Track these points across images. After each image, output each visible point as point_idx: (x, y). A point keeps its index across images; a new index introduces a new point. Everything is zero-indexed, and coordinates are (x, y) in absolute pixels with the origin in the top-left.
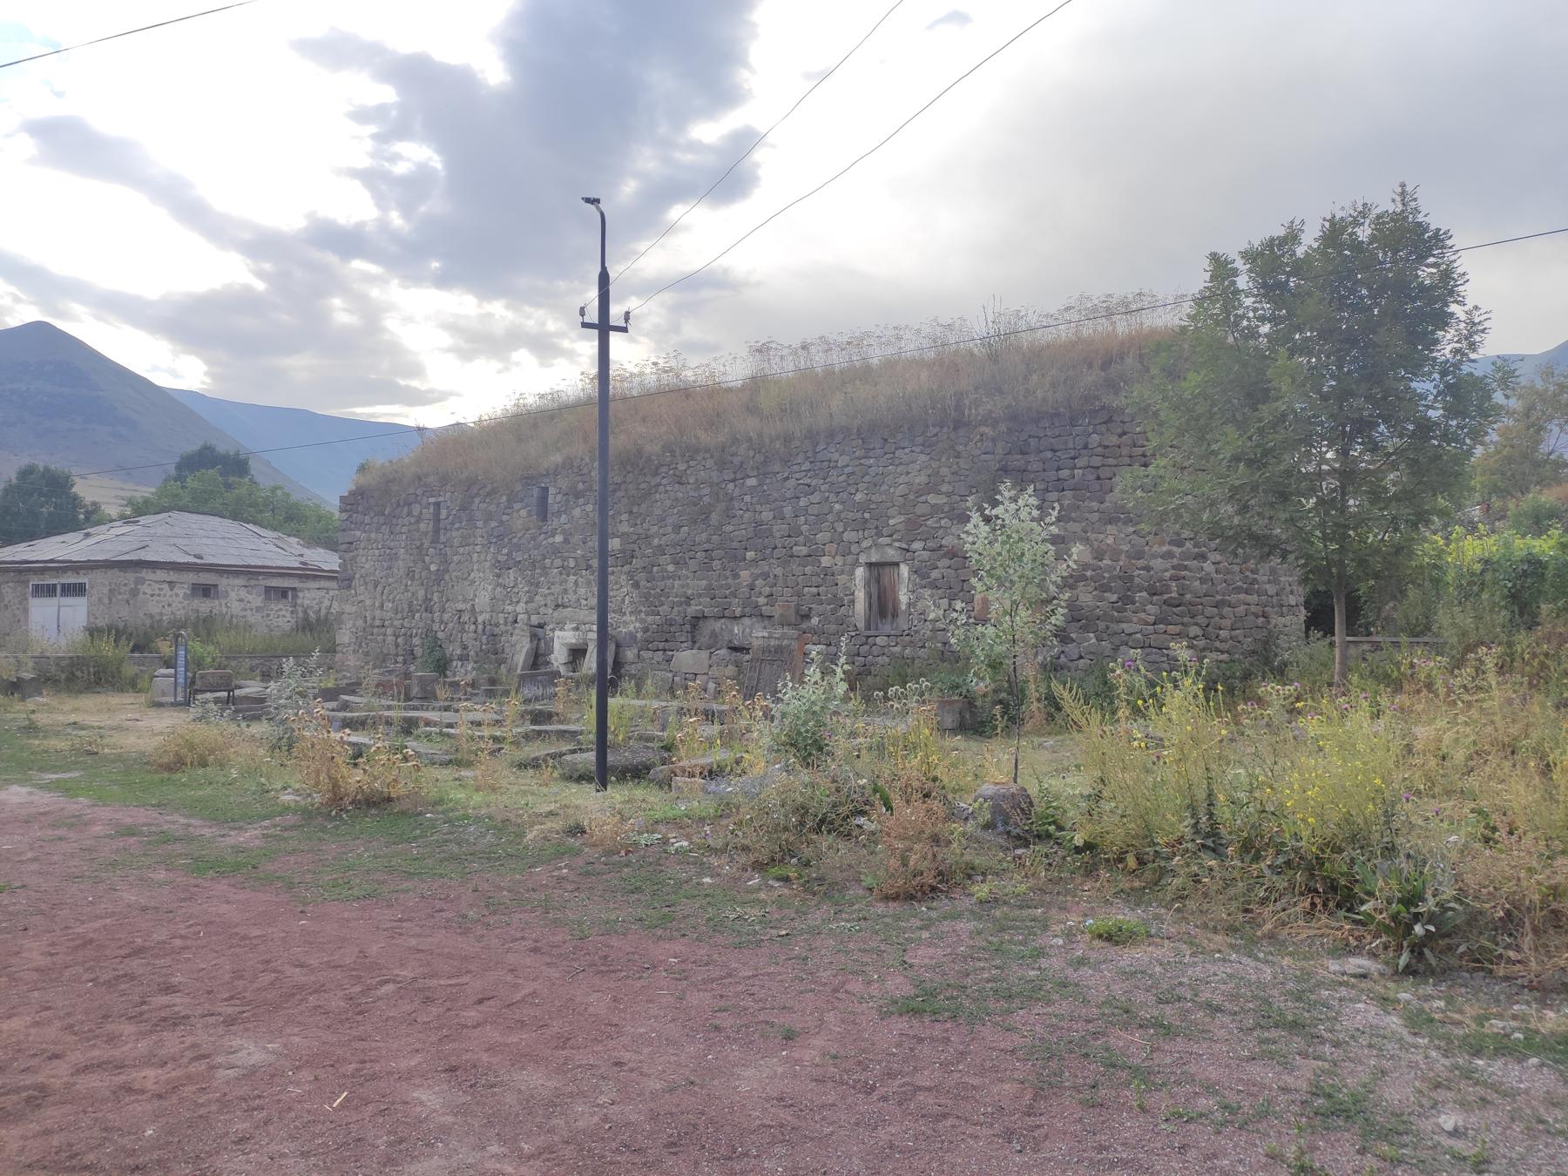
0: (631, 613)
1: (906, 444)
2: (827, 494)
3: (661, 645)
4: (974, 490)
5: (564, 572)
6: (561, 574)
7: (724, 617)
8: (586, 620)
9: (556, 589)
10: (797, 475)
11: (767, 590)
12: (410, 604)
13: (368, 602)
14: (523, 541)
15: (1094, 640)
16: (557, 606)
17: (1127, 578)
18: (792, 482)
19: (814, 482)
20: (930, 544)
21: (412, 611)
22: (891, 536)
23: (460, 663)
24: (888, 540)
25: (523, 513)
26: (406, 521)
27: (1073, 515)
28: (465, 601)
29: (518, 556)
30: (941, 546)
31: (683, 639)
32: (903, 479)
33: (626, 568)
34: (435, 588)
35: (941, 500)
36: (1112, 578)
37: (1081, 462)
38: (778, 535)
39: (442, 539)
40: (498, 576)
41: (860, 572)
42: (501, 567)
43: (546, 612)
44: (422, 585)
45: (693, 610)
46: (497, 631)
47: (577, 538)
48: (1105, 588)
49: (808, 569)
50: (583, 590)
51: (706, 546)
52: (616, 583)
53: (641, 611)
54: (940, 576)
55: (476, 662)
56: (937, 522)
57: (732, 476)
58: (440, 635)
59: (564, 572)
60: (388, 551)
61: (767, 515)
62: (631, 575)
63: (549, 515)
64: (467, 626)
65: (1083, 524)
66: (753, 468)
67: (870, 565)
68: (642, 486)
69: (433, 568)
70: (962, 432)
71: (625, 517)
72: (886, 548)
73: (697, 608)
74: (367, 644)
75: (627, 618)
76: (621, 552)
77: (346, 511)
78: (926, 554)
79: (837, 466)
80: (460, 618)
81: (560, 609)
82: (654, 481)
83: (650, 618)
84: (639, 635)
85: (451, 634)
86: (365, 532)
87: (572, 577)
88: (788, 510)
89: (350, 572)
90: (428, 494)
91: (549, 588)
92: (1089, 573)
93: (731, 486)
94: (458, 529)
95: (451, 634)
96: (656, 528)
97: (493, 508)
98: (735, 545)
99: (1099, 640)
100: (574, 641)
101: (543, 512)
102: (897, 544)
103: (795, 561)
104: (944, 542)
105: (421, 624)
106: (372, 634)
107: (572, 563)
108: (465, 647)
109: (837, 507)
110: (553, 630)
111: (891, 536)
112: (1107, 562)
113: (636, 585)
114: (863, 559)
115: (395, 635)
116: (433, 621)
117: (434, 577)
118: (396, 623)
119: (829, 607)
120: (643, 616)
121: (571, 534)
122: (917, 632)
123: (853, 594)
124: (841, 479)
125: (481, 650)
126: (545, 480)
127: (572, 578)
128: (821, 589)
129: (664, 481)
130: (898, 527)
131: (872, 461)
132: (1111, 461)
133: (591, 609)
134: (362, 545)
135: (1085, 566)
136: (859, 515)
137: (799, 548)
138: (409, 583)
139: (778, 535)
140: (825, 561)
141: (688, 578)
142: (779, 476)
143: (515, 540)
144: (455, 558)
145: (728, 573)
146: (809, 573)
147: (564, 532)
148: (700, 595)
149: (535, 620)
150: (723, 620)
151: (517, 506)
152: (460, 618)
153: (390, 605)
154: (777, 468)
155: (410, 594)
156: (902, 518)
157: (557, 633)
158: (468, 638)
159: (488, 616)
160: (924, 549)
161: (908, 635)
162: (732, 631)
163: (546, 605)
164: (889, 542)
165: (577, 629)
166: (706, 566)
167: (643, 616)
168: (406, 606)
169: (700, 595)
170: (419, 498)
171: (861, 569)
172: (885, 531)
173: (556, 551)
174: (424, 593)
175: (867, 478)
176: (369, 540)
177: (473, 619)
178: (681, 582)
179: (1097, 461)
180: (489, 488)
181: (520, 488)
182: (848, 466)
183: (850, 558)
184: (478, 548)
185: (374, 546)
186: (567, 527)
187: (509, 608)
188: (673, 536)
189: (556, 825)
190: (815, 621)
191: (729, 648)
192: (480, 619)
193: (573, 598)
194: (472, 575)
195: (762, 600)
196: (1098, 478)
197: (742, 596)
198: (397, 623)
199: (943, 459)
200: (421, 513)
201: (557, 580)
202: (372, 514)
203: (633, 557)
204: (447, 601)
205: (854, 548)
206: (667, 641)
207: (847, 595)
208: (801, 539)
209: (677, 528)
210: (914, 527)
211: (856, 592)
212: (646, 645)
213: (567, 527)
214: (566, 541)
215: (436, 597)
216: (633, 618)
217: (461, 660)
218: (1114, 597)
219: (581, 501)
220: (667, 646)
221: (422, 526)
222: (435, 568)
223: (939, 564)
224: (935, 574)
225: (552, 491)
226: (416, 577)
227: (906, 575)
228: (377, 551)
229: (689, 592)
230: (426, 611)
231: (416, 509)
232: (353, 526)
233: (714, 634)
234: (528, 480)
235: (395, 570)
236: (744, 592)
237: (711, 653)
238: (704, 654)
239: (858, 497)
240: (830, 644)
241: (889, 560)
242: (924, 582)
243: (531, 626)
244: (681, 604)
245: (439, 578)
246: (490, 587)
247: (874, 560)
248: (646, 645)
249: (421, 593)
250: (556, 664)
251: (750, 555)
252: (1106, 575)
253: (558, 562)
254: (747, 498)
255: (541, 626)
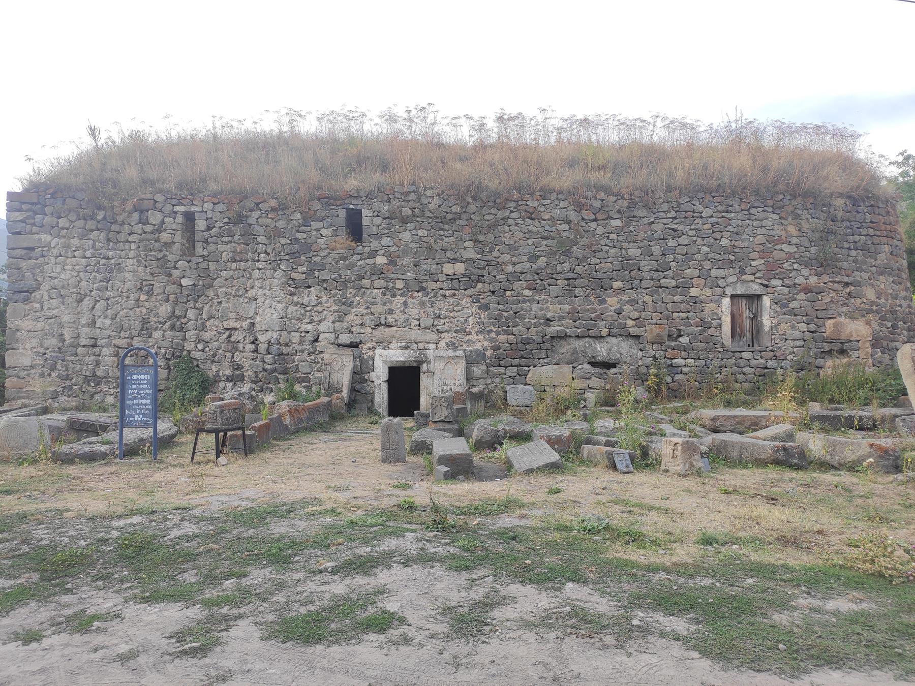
0: (477, 333)
1: (759, 204)
2: (695, 238)
3: (516, 362)
4: (813, 244)
5: (388, 292)
6: (385, 294)
7: (589, 336)
8: (419, 339)
9: (378, 309)
10: (665, 221)
11: (636, 315)
12: (145, 321)
13: (66, 318)
14: (329, 260)
15: (880, 354)
16: (380, 324)
17: (894, 312)
18: (658, 227)
19: (680, 228)
20: (787, 282)
21: (146, 328)
22: (754, 274)
23: (229, 385)
24: (752, 277)
25: (327, 232)
26: (138, 228)
27: (864, 267)
28: (239, 318)
29: (325, 275)
30: (795, 284)
31: (543, 356)
32: (759, 231)
33: (470, 292)
34: (191, 304)
35: (793, 249)
36: (887, 311)
37: (864, 231)
38: (645, 268)
39: (199, 250)
40: (292, 294)
41: (726, 301)
42: (294, 286)
43: (362, 330)
44: (167, 300)
45: (552, 330)
46: (285, 350)
47: (408, 261)
48: (883, 319)
49: (677, 298)
50: (415, 311)
51: (570, 275)
52: (457, 306)
53: (491, 331)
54: (799, 306)
55: (254, 382)
56: (790, 266)
57: (593, 217)
58: (196, 354)
59: (388, 292)
60: (103, 261)
61: (634, 252)
62: (475, 299)
63: (365, 237)
64: (241, 346)
65: (869, 274)
66: (619, 212)
67: (733, 297)
68: (487, 217)
69: (185, 282)
70: (799, 199)
71: (469, 244)
72: (751, 283)
73: (559, 329)
74: (66, 366)
75: (473, 337)
76: (463, 275)
77: (20, 210)
78: (786, 290)
79: (701, 217)
80: (230, 336)
81: (381, 328)
82: (500, 214)
83: (502, 338)
84: (488, 353)
85: (215, 355)
86: (59, 236)
87: (398, 297)
88: (656, 249)
89: (30, 282)
90: (174, 202)
91: (367, 308)
92: (874, 308)
93: (593, 225)
94: (226, 243)
95: (215, 355)
96: (508, 257)
97: (281, 224)
98: (601, 275)
99: (883, 353)
100: (403, 359)
101: (355, 230)
102: (759, 281)
103: (664, 291)
104: (796, 281)
105: (166, 343)
106: (76, 355)
107: (400, 284)
108: (239, 367)
109: (705, 249)
110: (373, 349)
111: (754, 274)
112: (883, 300)
113: (485, 307)
114: (729, 291)
115: (117, 355)
116: (184, 339)
117: (186, 292)
118: (116, 342)
119: (696, 329)
120: (493, 335)
121: (398, 257)
122: (780, 348)
123: (720, 319)
124: (705, 227)
125: (265, 370)
126: (355, 202)
127: (399, 299)
128: (691, 313)
129: (514, 215)
130: (760, 268)
131: (733, 215)
132: (878, 233)
133: (425, 328)
134: (55, 252)
135: (873, 303)
136: (726, 256)
137: (668, 281)
138: (143, 297)
139: (645, 268)
140: (694, 292)
141: (547, 303)
142: (646, 221)
143: (317, 259)
144: (224, 274)
145: (592, 299)
146: (679, 301)
147: (388, 254)
148: (563, 318)
149: (345, 339)
150: (587, 339)
151: (316, 225)
152: (230, 336)
153: (108, 322)
154: (641, 213)
155: (144, 311)
156: (763, 262)
157: (379, 351)
158: (244, 357)
159: (275, 335)
160: (783, 286)
161: (771, 351)
162: (596, 348)
163: (361, 325)
164: (753, 279)
165: (406, 348)
166: (569, 292)
167: (493, 335)
168: (137, 325)
169: (563, 318)
170: (159, 205)
171: (728, 299)
172: (748, 270)
173: (380, 273)
174: (169, 309)
175: (729, 228)
176: (67, 246)
177: (252, 339)
178: (539, 306)
179: (871, 232)
180: (273, 203)
181: (320, 206)
182: (712, 216)
183: (718, 290)
184: (260, 265)
185: (76, 254)
186: (392, 249)
187: (309, 327)
188: (529, 265)
189: (279, 535)
190: (684, 340)
191: (589, 363)
192: (262, 338)
193: (403, 317)
194: (251, 293)
195: (630, 323)
196: (872, 243)
197: (610, 319)
198: (122, 343)
199: (790, 219)
200: (163, 222)
201: (378, 300)
202: (73, 217)
203: (479, 281)
204: (209, 319)
205: (721, 283)
206: (522, 357)
207: (715, 319)
208: (670, 273)
209: (533, 258)
210: (773, 270)
211: (723, 318)
212: (498, 361)
213: (392, 249)
214: (392, 263)
215: (191, 314)
216: (481, 337)
217: (232, 381)
218: (889, 325)
219: (410, 226)
220: (522, 361)
221: (165, 236)
222: (191, 283)
223: (798, 297)
224: (793, 305)
225: (365, 212)
226: (156, 291)
227: (768, 304)
228: (84, 260)
229: (549, 315)
230: (173, 328)
231: (155, 218)
232: (35, 229)
233: (575, 352)
234: (329, 201)
235: (118, 283)
236: (612, 316)
237: (574, 368)
238: (567, 369)
239: (724, 242)
240: (699, 359)
241: (753, 292)
242: (784, 310)
243: (339, 345)
244: (539, 324)
245: (196, 293)
246: (280, 306)
247: (739, 292)
248: (498, 361)
249: (165, 310)
250: (377, 382)
251: (617, 285)
252: (883, 309)
253: (382, 283)
254: (613, 236)
255: (354, 345)
